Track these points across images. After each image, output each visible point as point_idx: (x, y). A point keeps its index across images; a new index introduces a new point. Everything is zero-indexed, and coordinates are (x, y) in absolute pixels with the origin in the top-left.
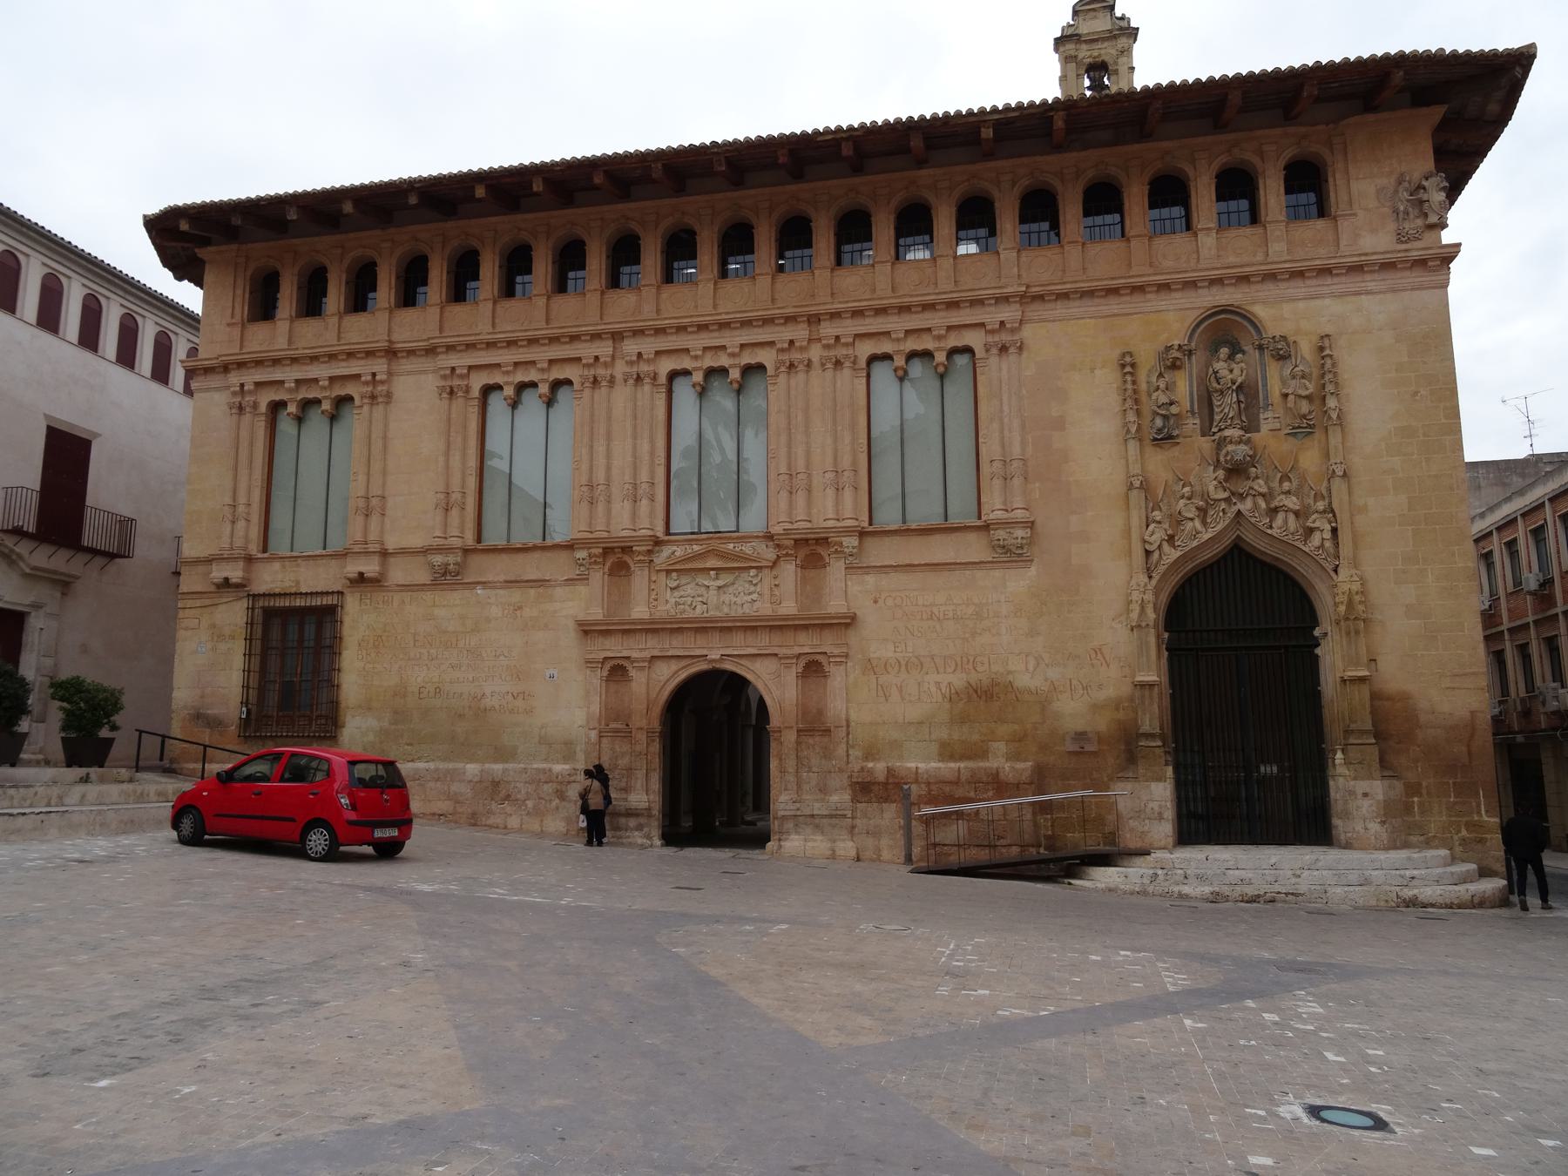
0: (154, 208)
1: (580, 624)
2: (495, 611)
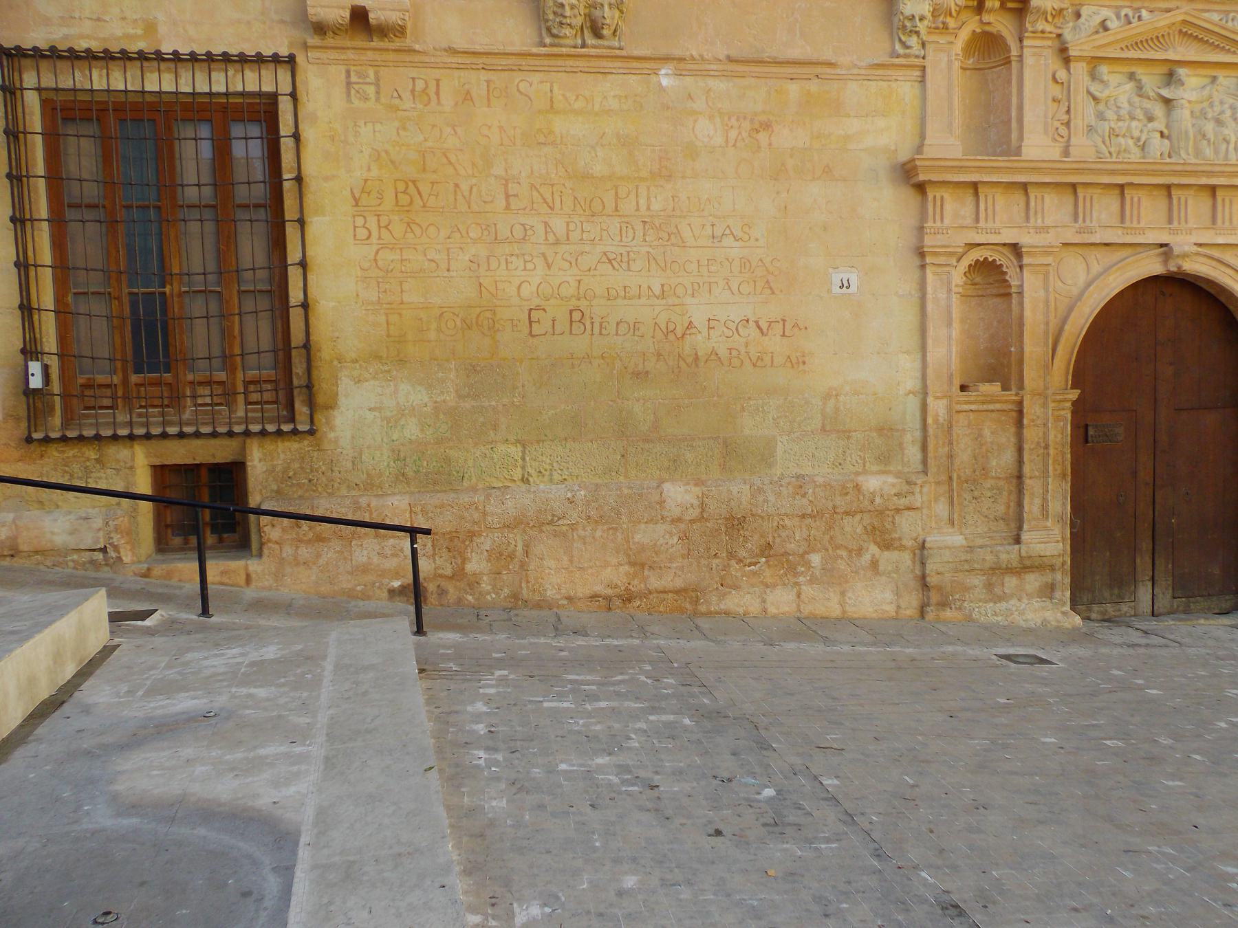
2: (706, 130)
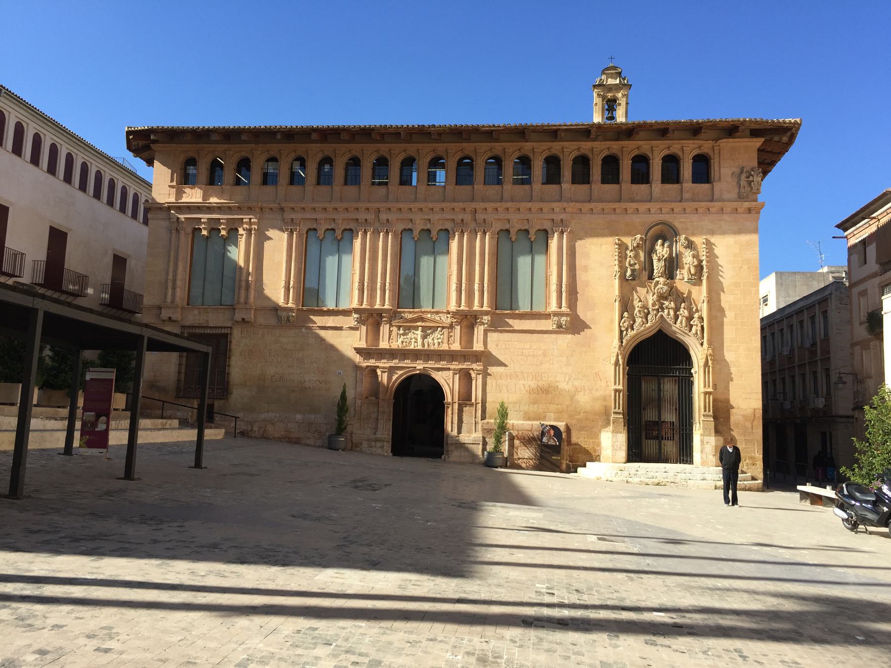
0: (141, 125)
1: (355, 349)
